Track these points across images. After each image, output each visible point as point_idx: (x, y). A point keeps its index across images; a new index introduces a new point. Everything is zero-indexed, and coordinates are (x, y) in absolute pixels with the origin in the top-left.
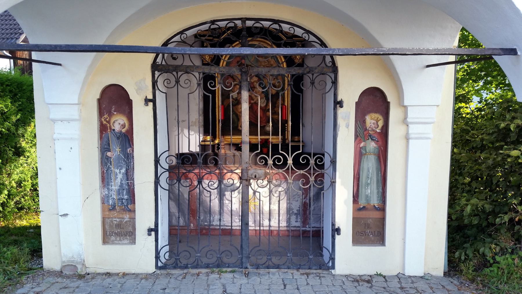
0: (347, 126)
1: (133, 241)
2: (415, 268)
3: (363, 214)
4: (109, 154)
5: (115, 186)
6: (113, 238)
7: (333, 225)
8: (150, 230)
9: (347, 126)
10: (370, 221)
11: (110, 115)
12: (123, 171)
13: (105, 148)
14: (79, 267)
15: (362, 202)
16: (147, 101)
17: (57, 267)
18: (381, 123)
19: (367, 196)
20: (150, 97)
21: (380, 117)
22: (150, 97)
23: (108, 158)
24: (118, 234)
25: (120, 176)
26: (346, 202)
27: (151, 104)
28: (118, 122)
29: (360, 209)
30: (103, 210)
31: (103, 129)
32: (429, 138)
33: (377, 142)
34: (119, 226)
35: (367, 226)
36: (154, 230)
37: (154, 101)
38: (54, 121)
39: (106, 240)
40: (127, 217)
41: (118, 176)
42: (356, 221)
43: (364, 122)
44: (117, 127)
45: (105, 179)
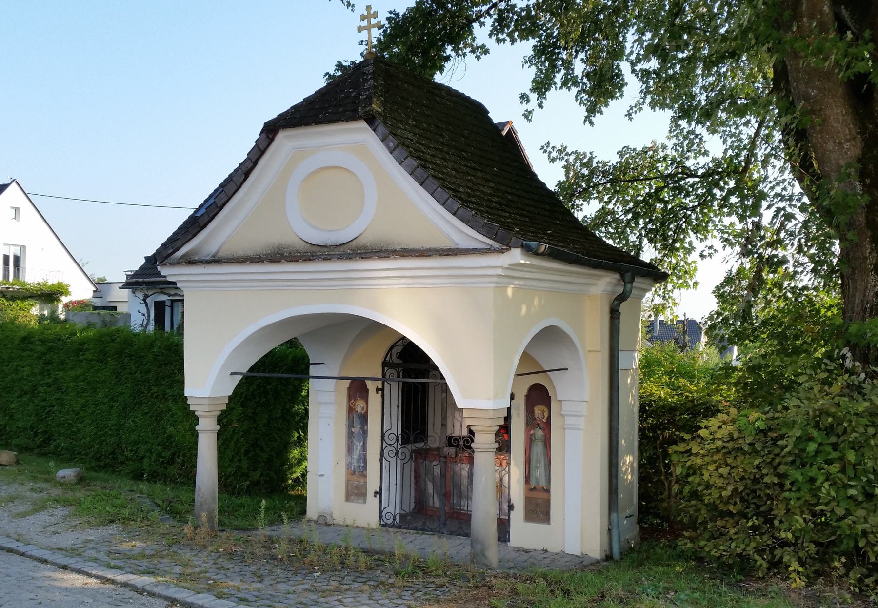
0: (518, 415)
1: (365, 502)
2: (573, 548)
3: (534, 494)
4: (353, 430)
5: (356, 456)
6: (353, 497)
7: (509, 501)
8: (376, 493)
9: (518, 415)
10: (539, 501)
11: (355, 400)
12: (362, 443)
13: (351, 425)
14: (328, 518)
15: (533, 484)
16: (378, 390)
17: (315, 518)
18: (546, 414)
19: (537, 478)
20: (380, 387)
21: (546, 409)
22: (380, 387)
23: (352, 433)
24: (356, 495)
25: (359, 448)
26: (518, 481)
27: (380, 392)
28: (360, 405)
29: (532, 490)
30: (347, 474)
31: (351, 410)
32: (579, 429)
33: (544, 430)
34: (357, 487)
35: (537, 505)
36: (379, 493)
37: (383, 390)
38: (320, 403)
39: (348, 499)
40: (362, 481)
41: (358, 445)
42: (528, 501)
43: (533, 412)
44: (359, 410)
45: (350, 449)
